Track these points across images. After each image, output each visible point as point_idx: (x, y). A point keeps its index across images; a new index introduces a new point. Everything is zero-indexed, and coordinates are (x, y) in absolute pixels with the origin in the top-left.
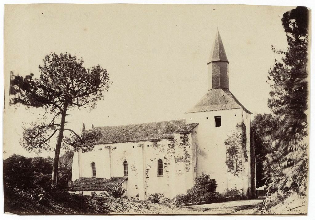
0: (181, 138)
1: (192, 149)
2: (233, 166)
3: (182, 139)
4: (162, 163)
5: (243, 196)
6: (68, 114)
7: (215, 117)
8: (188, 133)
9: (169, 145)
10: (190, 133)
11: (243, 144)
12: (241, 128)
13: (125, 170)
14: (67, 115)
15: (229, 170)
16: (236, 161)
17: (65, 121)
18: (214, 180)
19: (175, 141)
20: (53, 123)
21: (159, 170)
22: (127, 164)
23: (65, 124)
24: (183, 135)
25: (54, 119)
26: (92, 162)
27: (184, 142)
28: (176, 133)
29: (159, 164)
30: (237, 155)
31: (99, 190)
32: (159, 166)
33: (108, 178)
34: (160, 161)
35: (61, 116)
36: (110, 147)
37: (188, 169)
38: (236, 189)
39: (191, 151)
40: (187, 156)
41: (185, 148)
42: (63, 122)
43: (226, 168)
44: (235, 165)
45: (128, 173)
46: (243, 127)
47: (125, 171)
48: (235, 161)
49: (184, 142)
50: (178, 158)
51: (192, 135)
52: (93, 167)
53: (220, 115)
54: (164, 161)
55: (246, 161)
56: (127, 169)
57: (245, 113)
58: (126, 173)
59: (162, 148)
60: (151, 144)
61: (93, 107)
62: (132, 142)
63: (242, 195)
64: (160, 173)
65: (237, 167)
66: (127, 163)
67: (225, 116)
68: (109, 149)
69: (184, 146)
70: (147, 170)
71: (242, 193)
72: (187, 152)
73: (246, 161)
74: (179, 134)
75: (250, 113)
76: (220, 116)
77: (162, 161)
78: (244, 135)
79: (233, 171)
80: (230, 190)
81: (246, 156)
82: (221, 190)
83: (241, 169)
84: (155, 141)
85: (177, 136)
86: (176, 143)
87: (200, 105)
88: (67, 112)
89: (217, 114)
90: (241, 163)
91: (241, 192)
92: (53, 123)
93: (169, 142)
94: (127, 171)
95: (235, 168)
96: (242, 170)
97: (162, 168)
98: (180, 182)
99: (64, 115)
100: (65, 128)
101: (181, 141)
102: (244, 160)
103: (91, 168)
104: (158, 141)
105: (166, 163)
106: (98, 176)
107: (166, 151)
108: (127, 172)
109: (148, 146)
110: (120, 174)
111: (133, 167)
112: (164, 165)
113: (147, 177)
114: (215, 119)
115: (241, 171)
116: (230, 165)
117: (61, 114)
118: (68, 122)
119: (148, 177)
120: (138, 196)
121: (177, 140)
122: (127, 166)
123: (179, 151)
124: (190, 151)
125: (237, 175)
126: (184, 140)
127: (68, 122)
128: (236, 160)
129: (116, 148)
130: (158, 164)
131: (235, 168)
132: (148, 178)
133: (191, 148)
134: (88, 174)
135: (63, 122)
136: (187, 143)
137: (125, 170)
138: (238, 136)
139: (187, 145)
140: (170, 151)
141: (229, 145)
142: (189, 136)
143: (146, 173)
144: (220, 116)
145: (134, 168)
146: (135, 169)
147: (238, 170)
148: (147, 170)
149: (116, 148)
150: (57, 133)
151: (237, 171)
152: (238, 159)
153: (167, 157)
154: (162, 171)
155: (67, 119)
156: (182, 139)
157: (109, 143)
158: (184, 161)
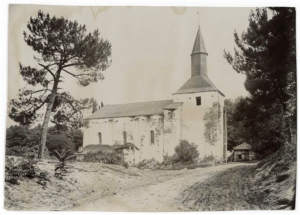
4: (153, 133)
7: (196, 97)
9: (159, 119)
21: (151, 139)
26: (98, 132)
27: (171, 117)
28: (165, 109)
29: (151, 135)
34: (152, 132)
38: (212, 156)
41: (171, 121)
44: (211, 136)
48: (212, 133)
50: (166, 130)
51: (178, 111)
54: (155, 132)
59: (153, 122)
60: (144, 118)
64: (152, 141)
65: (213, 137)
70: (142, 139)
74: (168, 110)
76: (200, 97)
77: (153, 132)
80: (207, 156)
82: (201, 156)
84: (148, 116)
85: (166, 112)
87: (184, 87)
89: (198, 95)
93: (159, 117)
95: (212, 139)
97: (154, 138)
98: (168, 147)
103: (98, 137)
104: (150, 116)
105: (156, 134)
106: (103, 144)
107: (157, 124)
109: (143, 120)
114: (196, 99)
115: (217, 141)
116: (207, 135)
119: (143, 145)
120: (134, 160)
125: (213, 145)
126: (171, 115)
128: (213, 132)
129: (117, 121)
130: (150, 135)
136: (173, 118)
141: (207, 121)
144: (200, 97)
145: (132, 137)
149: (117, 121)
151: (213, 141)
152: (214, 131)
153: (158, 129)
156: (170, 115)
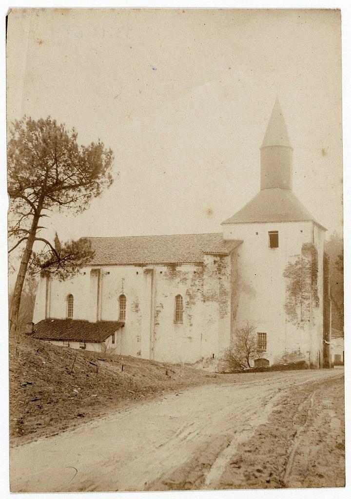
0: (215, 262)
1: (231, 282)
2: (295, 313)
3: (217, 265)
5: (311, 364)
6: (43, 215)
7: (269, 232)
8: (226, 255)
9: (195, 272)
10: (230, 256)
11: (312, 277)
12: (309, 252)
13: (121, 310)
14: (41, 216)
15: (289, 319)
16: (301, 305)
17: (38, 225)
18: (264, 334)
19: (206, 266)
20: (19, 227)
21: (177, 312)
22: (125, 300)
23: (37, 230)
24: (218, 259)
25: (20, 221)
27: (219, 270)
28: (207, 254)
30: (303, 294)
31: (76, 341)
32: (177, 306)
33: (93, 320)
35: (32, 217)
36: (99, 270)
37: (222, 315)
39: (229, 284)
40: (223, 293)
42: (35, 227)
43: (285, 316)
44: (298, 311)
45: (126, 315)
46: (314, 253)
47: (121, 311)
49: (219, 270)
52: (69, 302)
53: (277, 230)
54: (185, 299)
55: (317, 305)
56: (125, 308)
57: (316, 229)
58: (122, 315)
61: (81, 209)
62: (136, 265)
63: (308, 362)
64: (178, 317)
66: (125, 298)
67: (285, 230)
68: (98, 274)
69: (219, 276)
71: (309, 358)
72: (224, 285)
73: (317, 305)
75: (325, 230)
76: (277, 232)
77: (182, 298)
78: (314, 264)
79: (295, 321)
81: (317, 298)
83: (308, 319)
85: (209, 260)
86: (206, 270)
88: (43, 212)
89: (273, 227)
90: (308, 309)
91: (307, 356)
92: (19, 227)
94: (125, 311)
95: (299, 316)
96: (310, 320)
99: (37, 216)
100: (37, 236)
101: (214, 268)
102: (314, 304)
106: (77, 316)
107: (189, 282)
108: (125, 314)
110: (111, 314)
111: (134, 306)
112: (184, 305)
113: (156, 322)
115: (309, 321)
117: (33, 214)
118: (43, 227)
121: (209, 266)
122: (125, 303)
123: (210, 284)
124: (227, 286)
125: (302, 328)
126: (220, 266)
127: (43, 227)
129: (109, 273)
131: (299, 316)
132: (158, 326)
133: (229, 280)
134: (59, 312)
135: (35, 227)
136: (223, 271)
137: (121, 310)
138: (306, 264)
139: (223, 275)
140: (197, 283)
142: (228, 259)
143: (156, 317)
144: (277, 232)
145: (137, 307)
146: (137, 309)
147: (303, 319)
148: (157, 311)
149: (109, 273)
150: (24, 244)
152: (305, 301)
154: (182, 315)
155: (41, 222)
156: (217, 265)
157: (98, 265)
158: (216, 300)
